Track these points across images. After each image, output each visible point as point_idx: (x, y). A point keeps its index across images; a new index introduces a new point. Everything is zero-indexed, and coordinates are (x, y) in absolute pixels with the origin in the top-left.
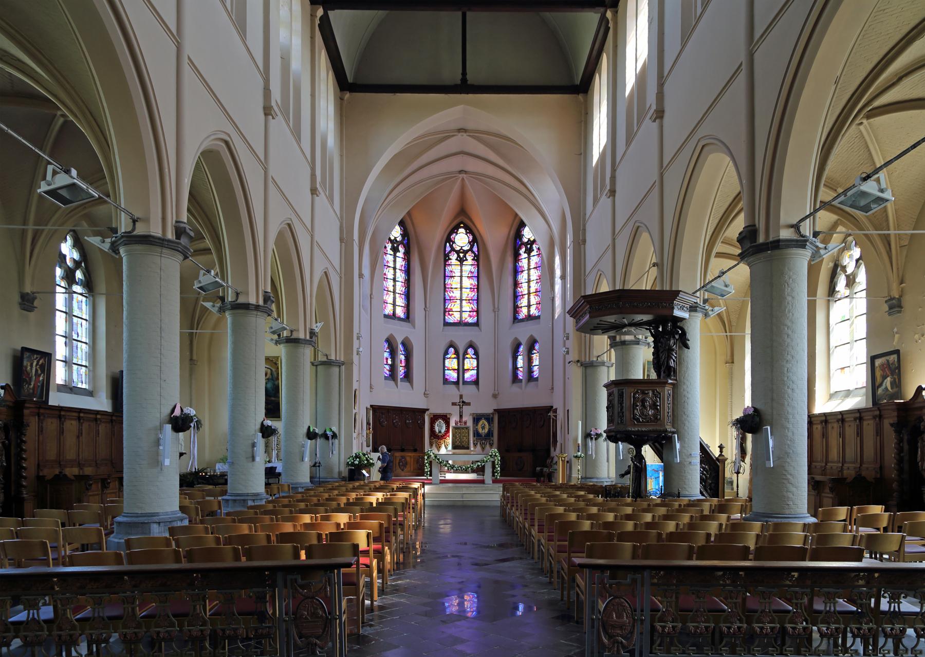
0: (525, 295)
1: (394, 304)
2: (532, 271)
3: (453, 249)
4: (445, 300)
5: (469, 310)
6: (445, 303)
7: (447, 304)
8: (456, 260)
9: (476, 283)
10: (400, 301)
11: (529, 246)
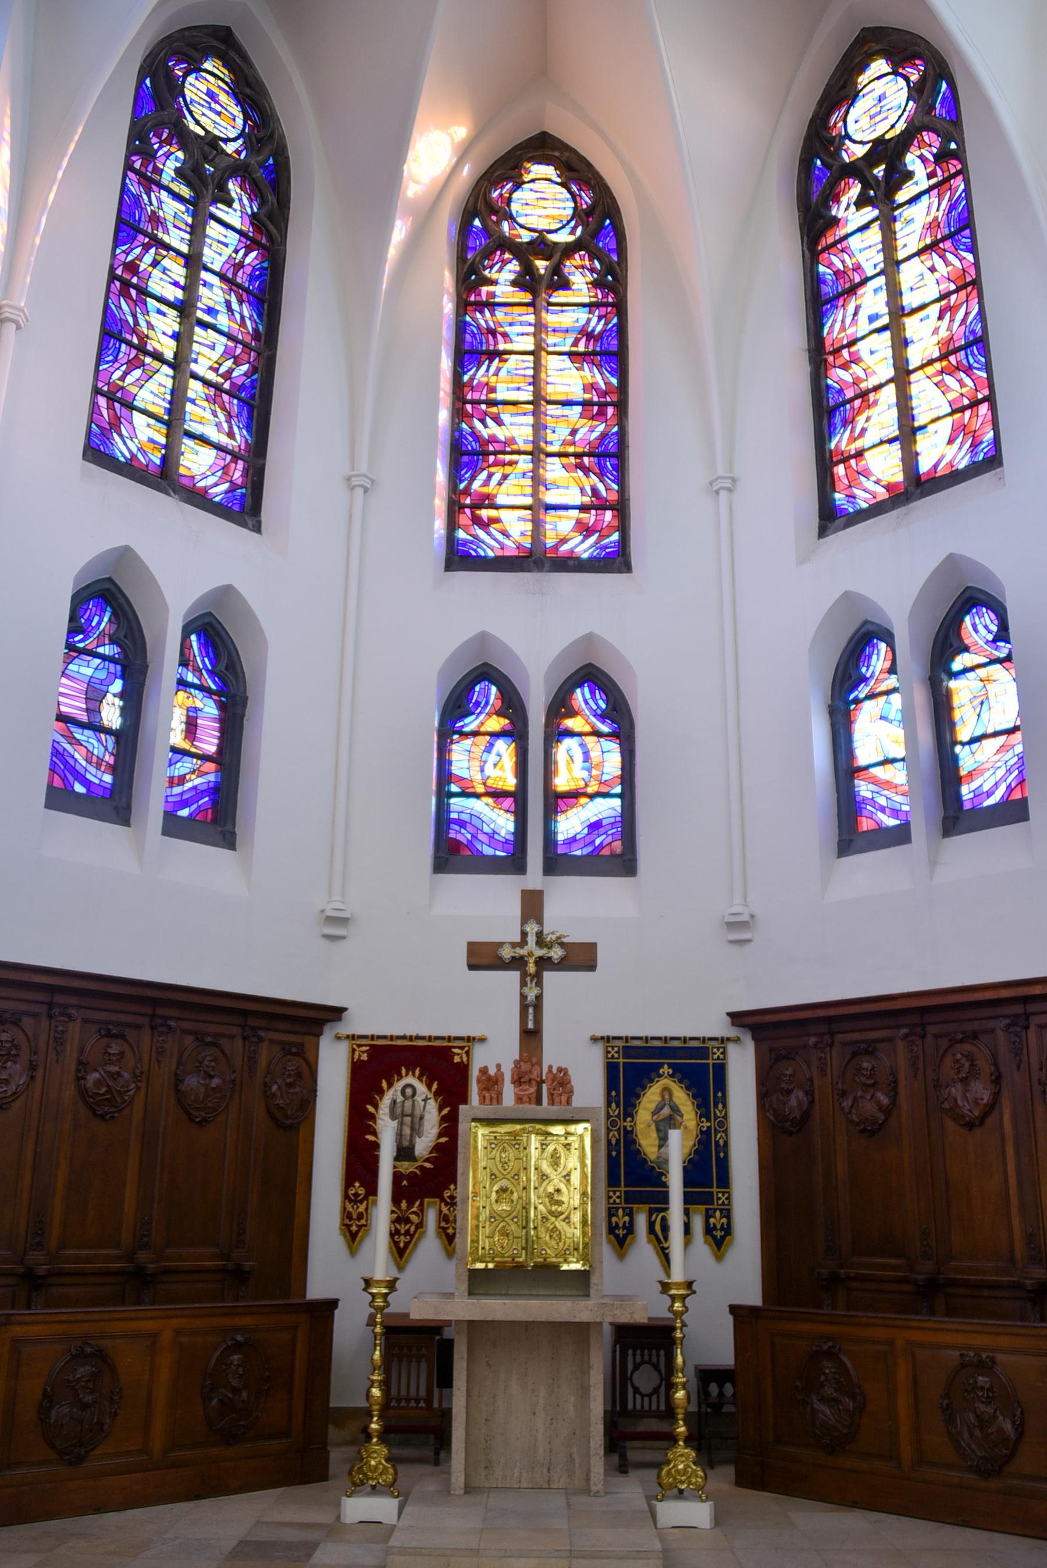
0: (877, 388)
2: (909, 273)
5: (577, 499)
8: (514, 283)
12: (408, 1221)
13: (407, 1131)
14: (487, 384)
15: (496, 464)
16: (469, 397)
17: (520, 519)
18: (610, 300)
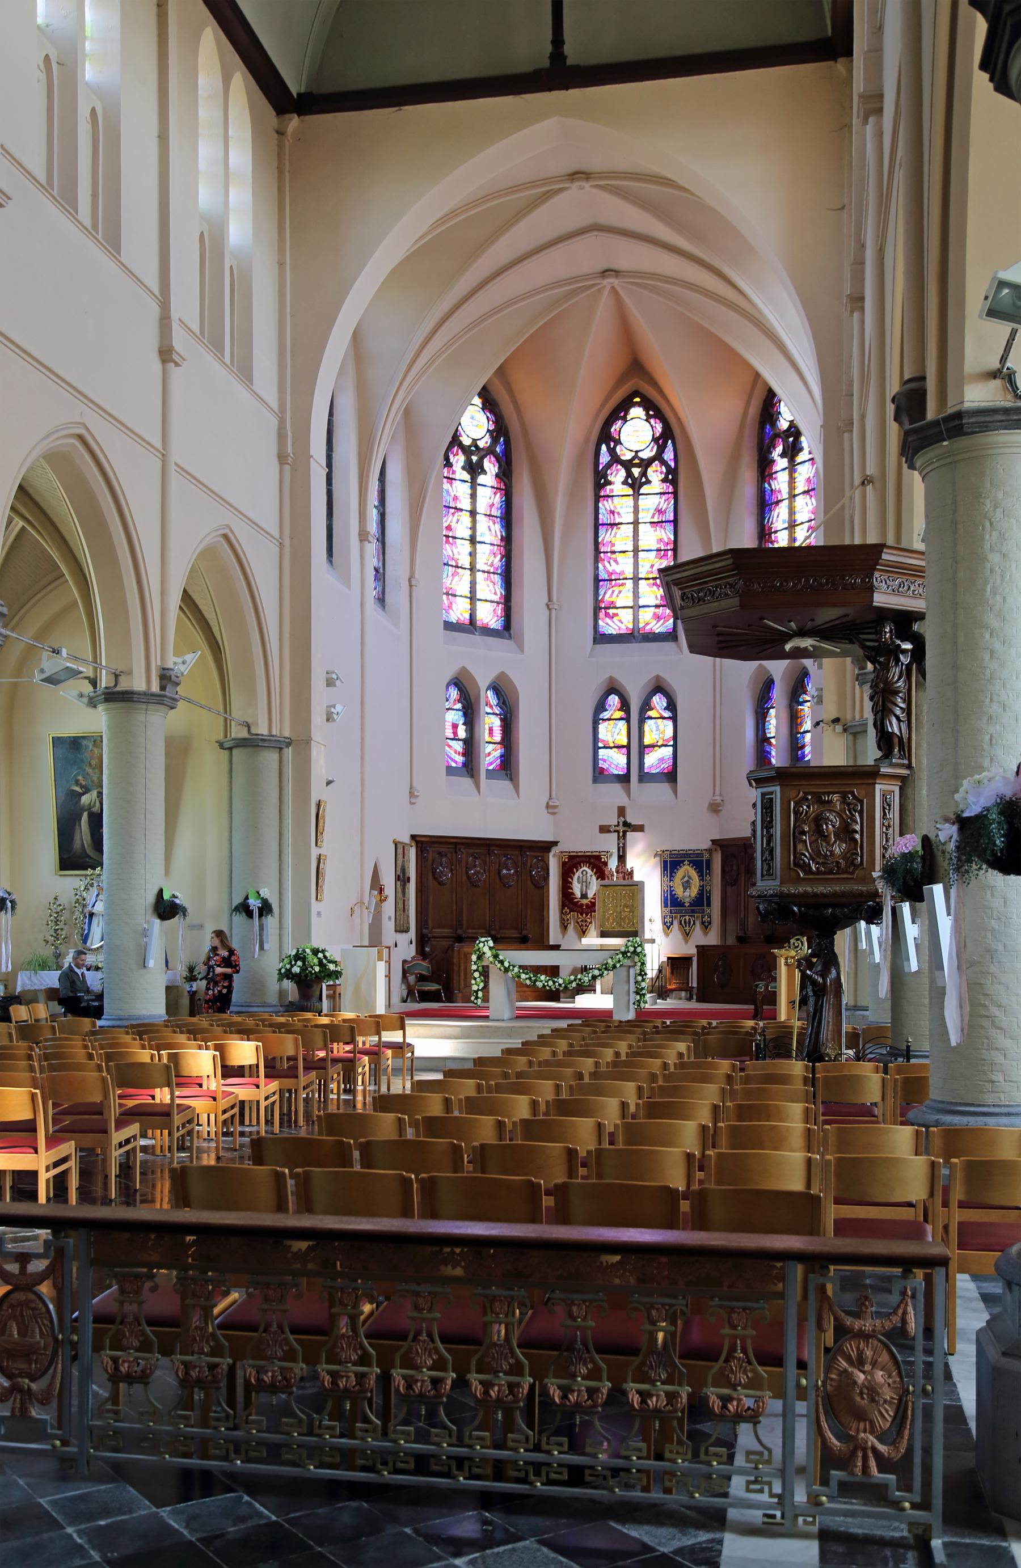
1: (473, 598)
3: (615, 459)
4: (597, 580)
6: (597, 588)
7: (601, 592)
9: (672, 537)
10: (490, 589)
11: (791, 439)
12: (586, 921)
13: (584, 888)
15: (615, 585)
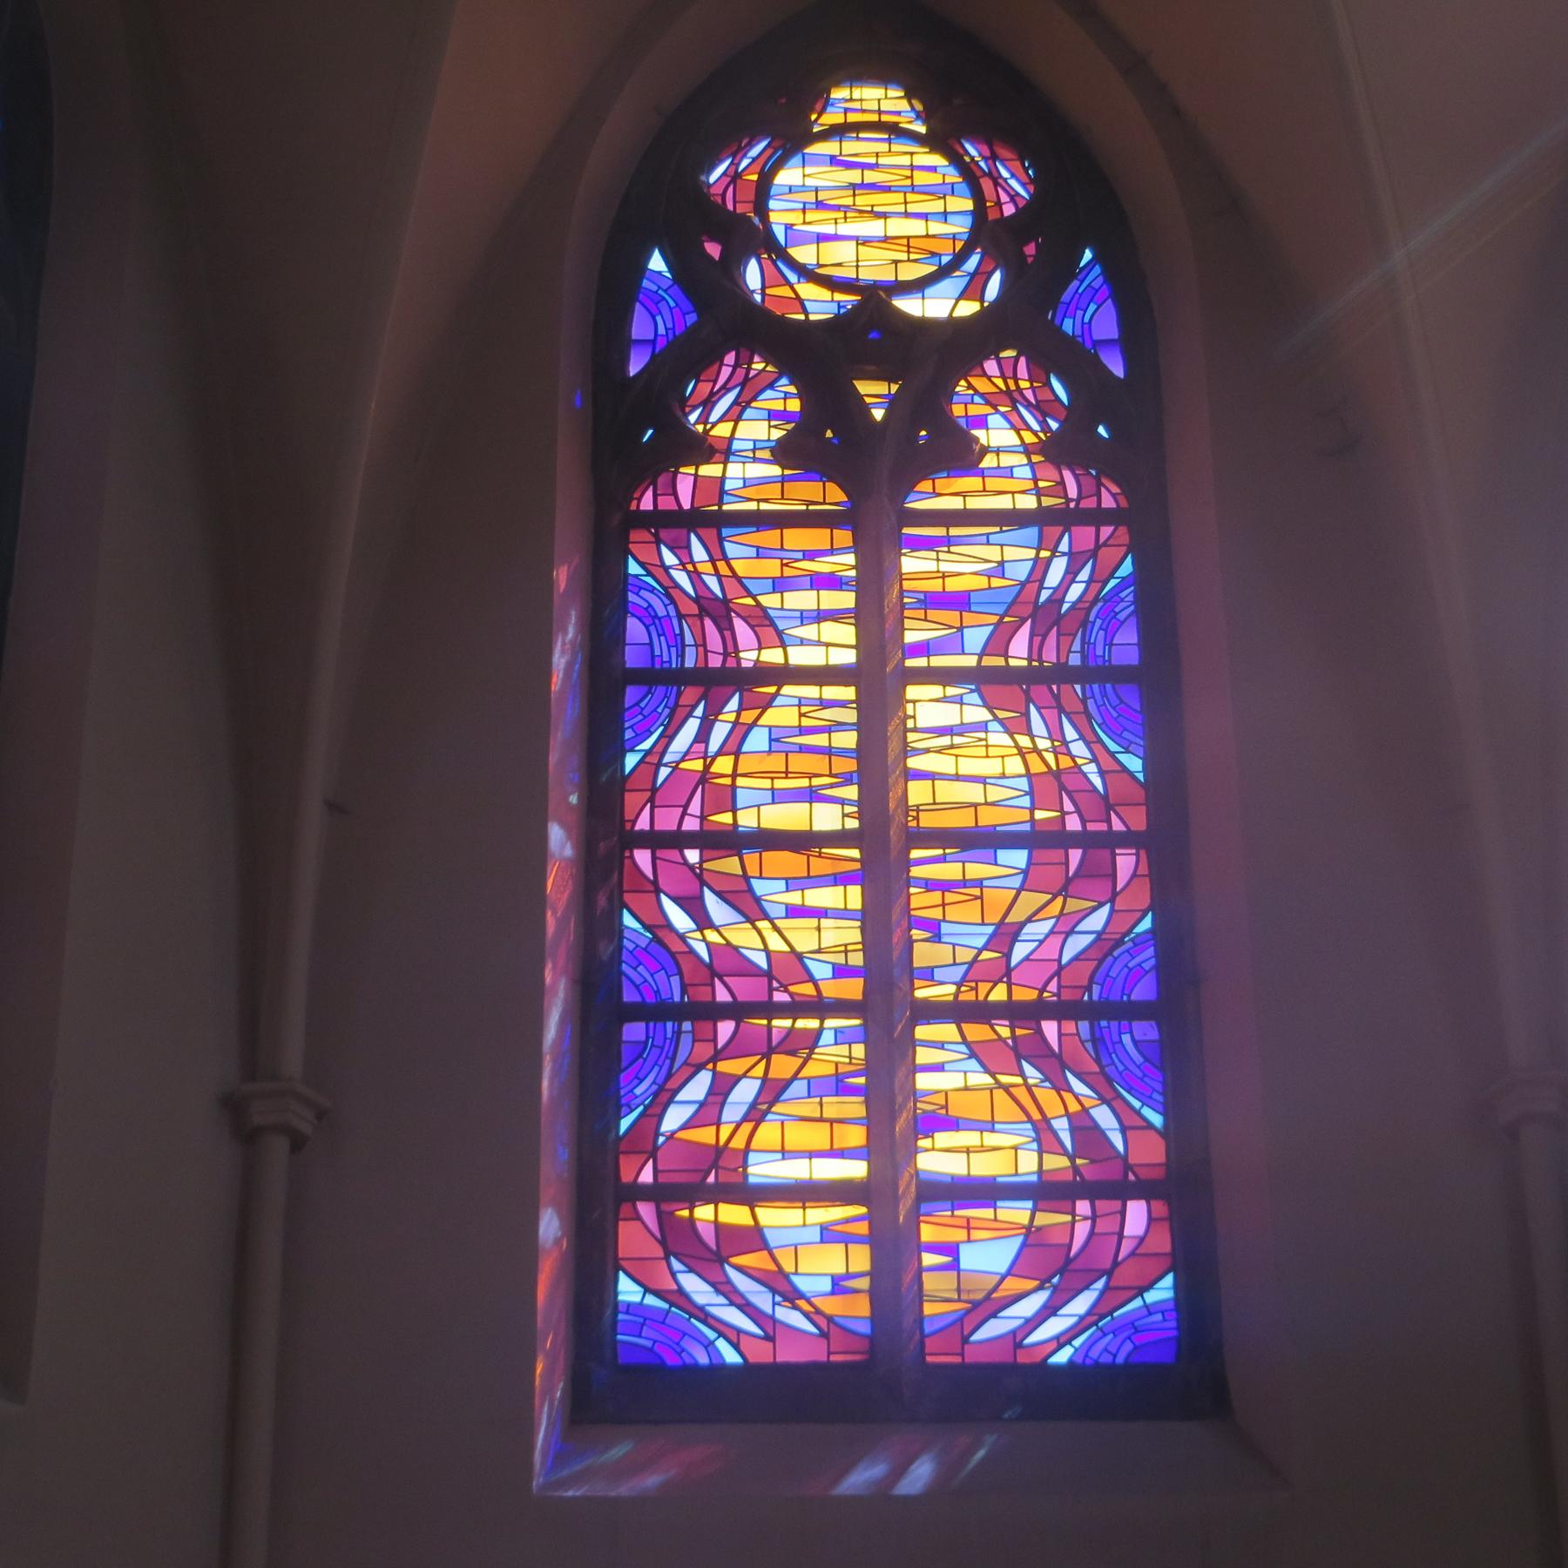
8: (782, 453)
14: (705, 777)
15: (734, 1049)
16: (643, 824)
17: (828, 1234)
18: (1108, 502)
